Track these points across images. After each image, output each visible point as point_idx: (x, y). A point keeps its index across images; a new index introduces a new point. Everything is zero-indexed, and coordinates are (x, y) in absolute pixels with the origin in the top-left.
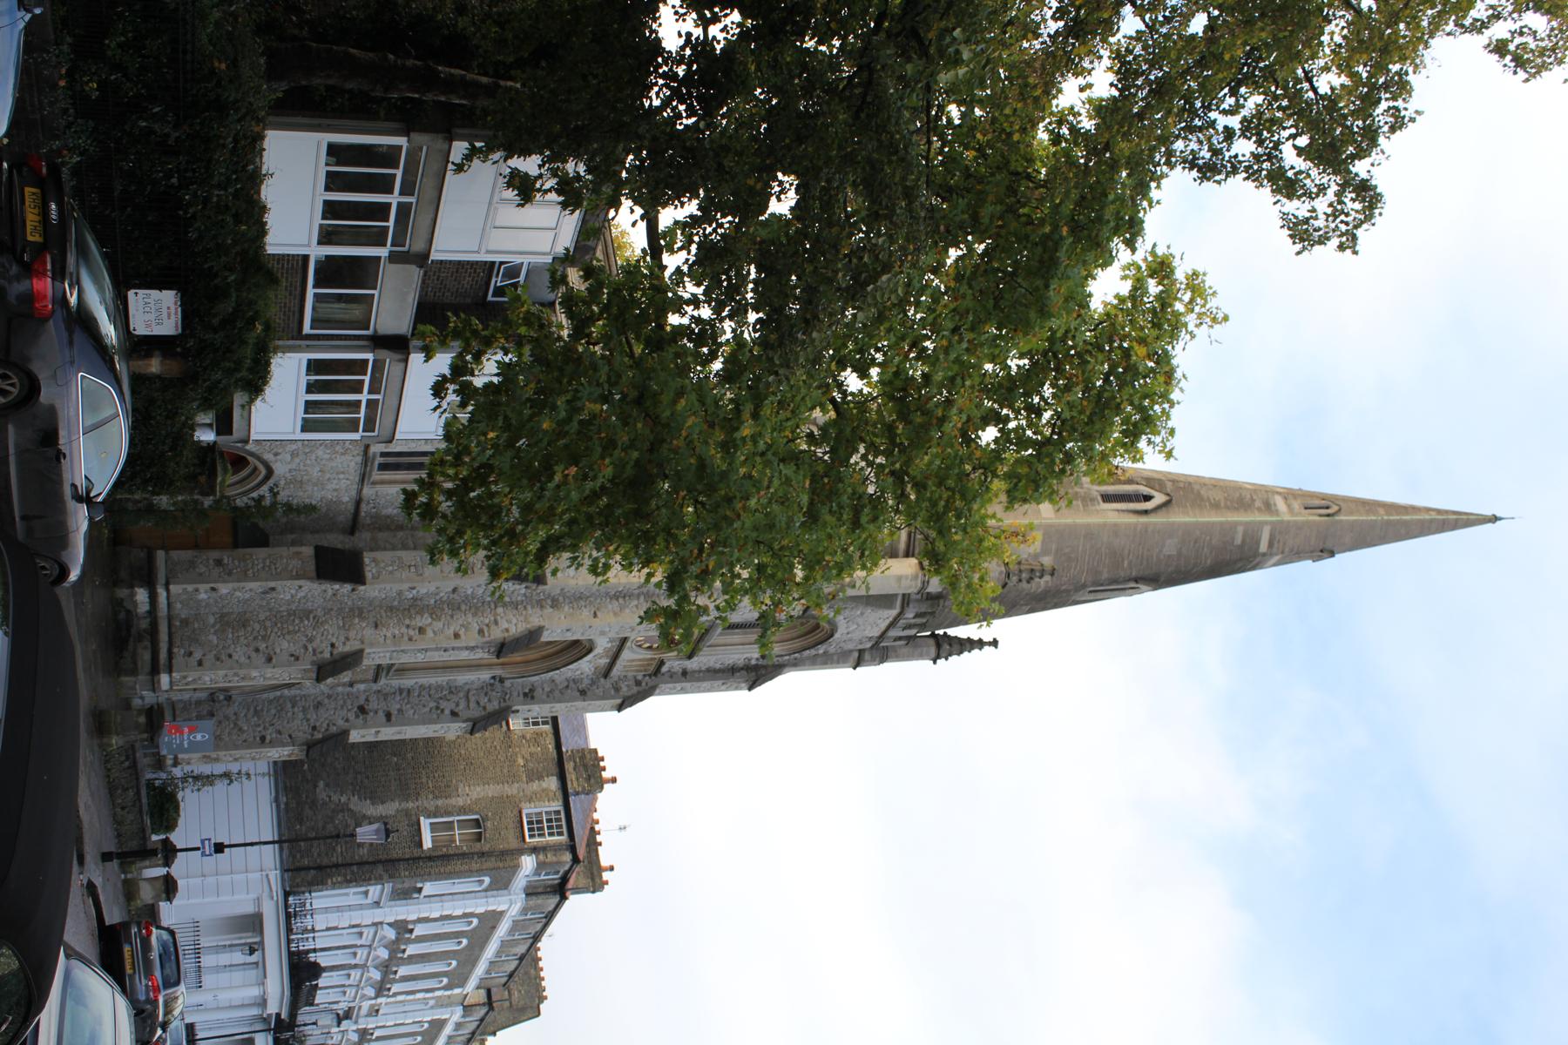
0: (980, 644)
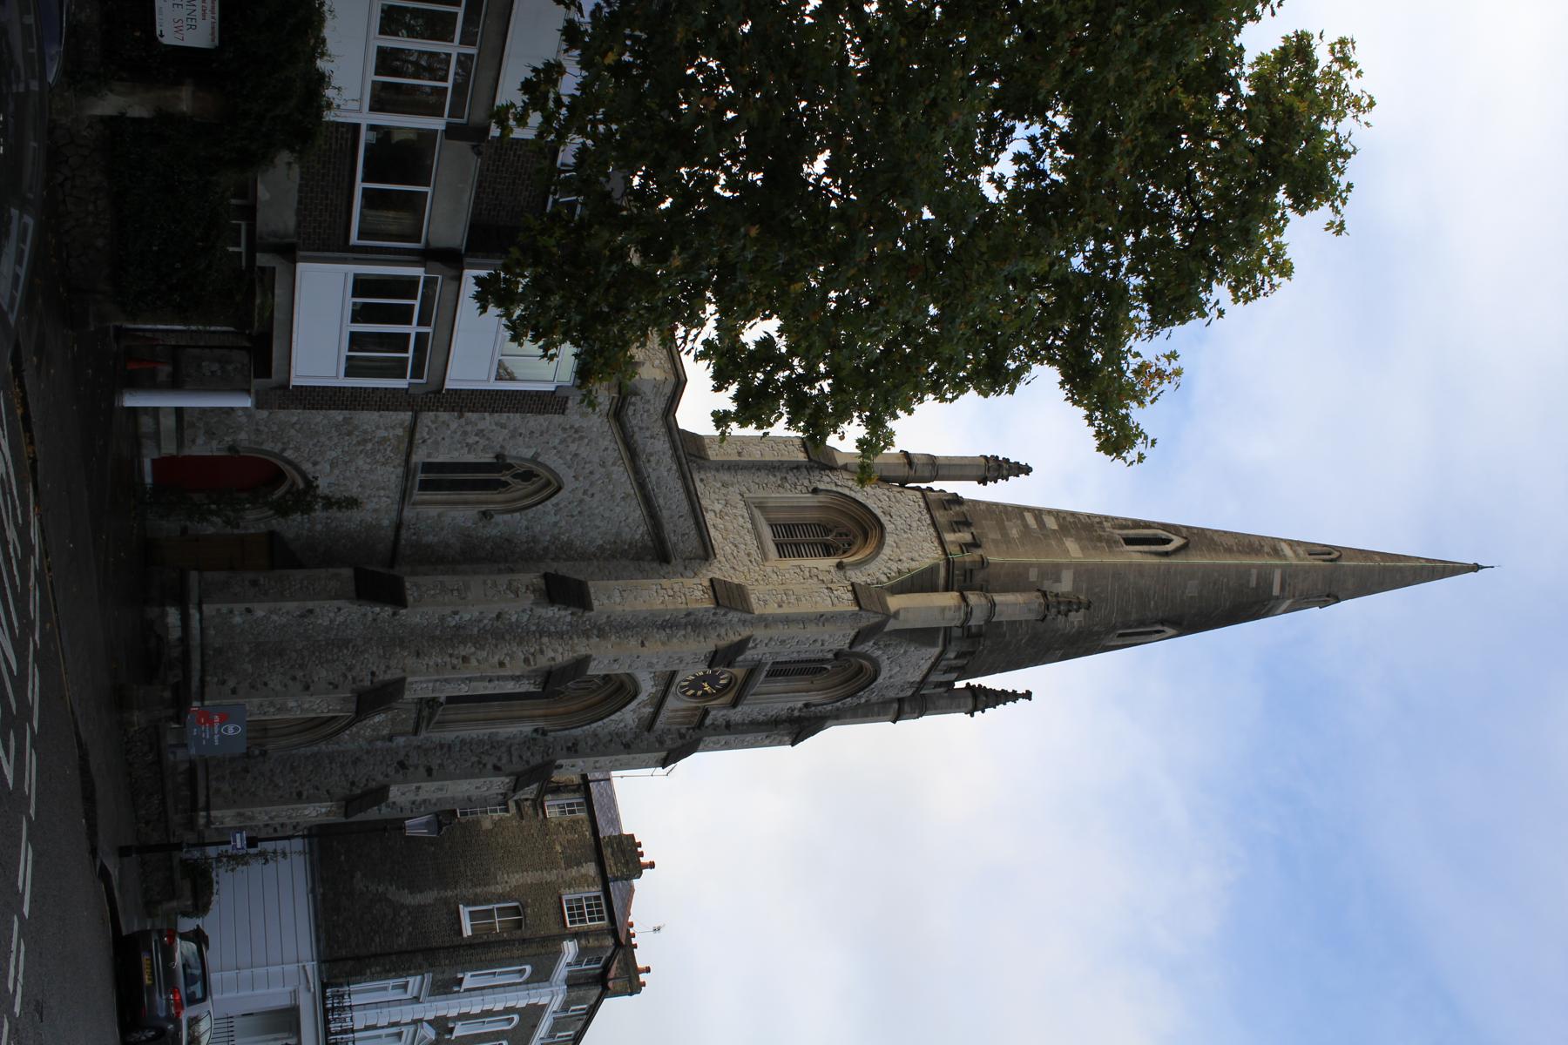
0: (1013, 696)
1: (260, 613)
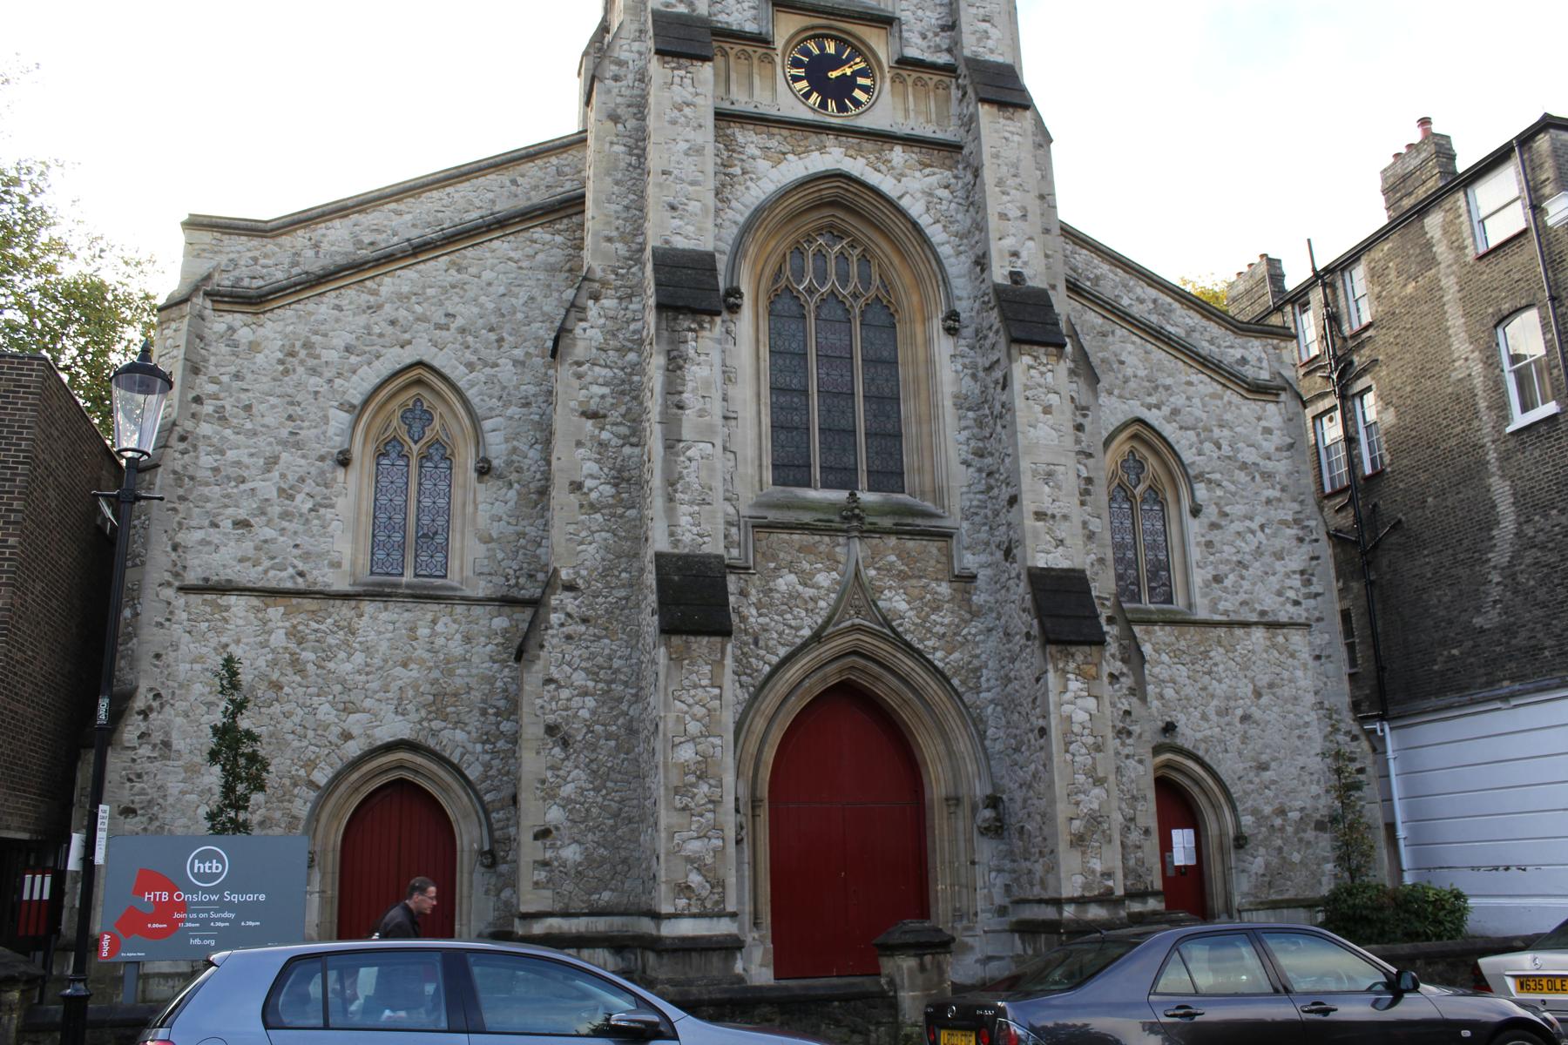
1: (555, 815)
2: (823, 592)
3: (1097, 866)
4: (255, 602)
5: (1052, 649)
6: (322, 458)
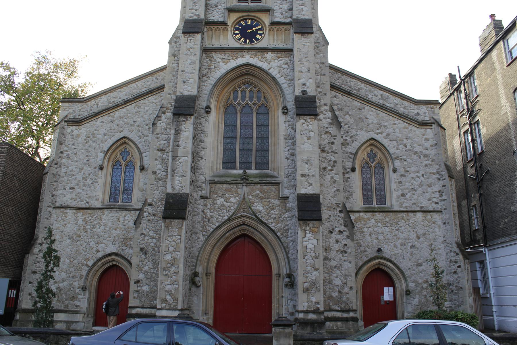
1: (141, 276)
2: (233, 204)
3: (314, 300)
4: (74, 211)
5: (301, 222)
6: (95, 168)
